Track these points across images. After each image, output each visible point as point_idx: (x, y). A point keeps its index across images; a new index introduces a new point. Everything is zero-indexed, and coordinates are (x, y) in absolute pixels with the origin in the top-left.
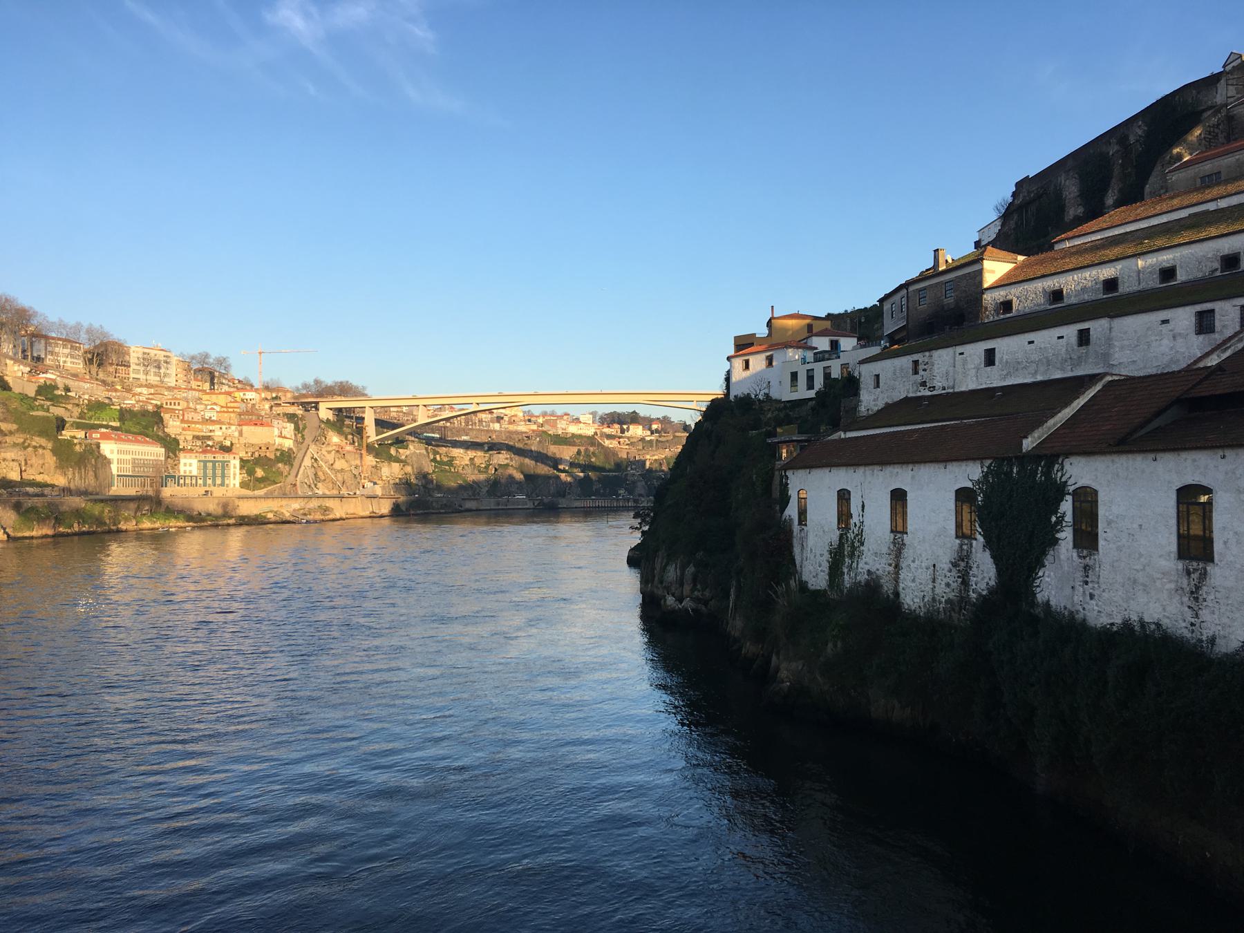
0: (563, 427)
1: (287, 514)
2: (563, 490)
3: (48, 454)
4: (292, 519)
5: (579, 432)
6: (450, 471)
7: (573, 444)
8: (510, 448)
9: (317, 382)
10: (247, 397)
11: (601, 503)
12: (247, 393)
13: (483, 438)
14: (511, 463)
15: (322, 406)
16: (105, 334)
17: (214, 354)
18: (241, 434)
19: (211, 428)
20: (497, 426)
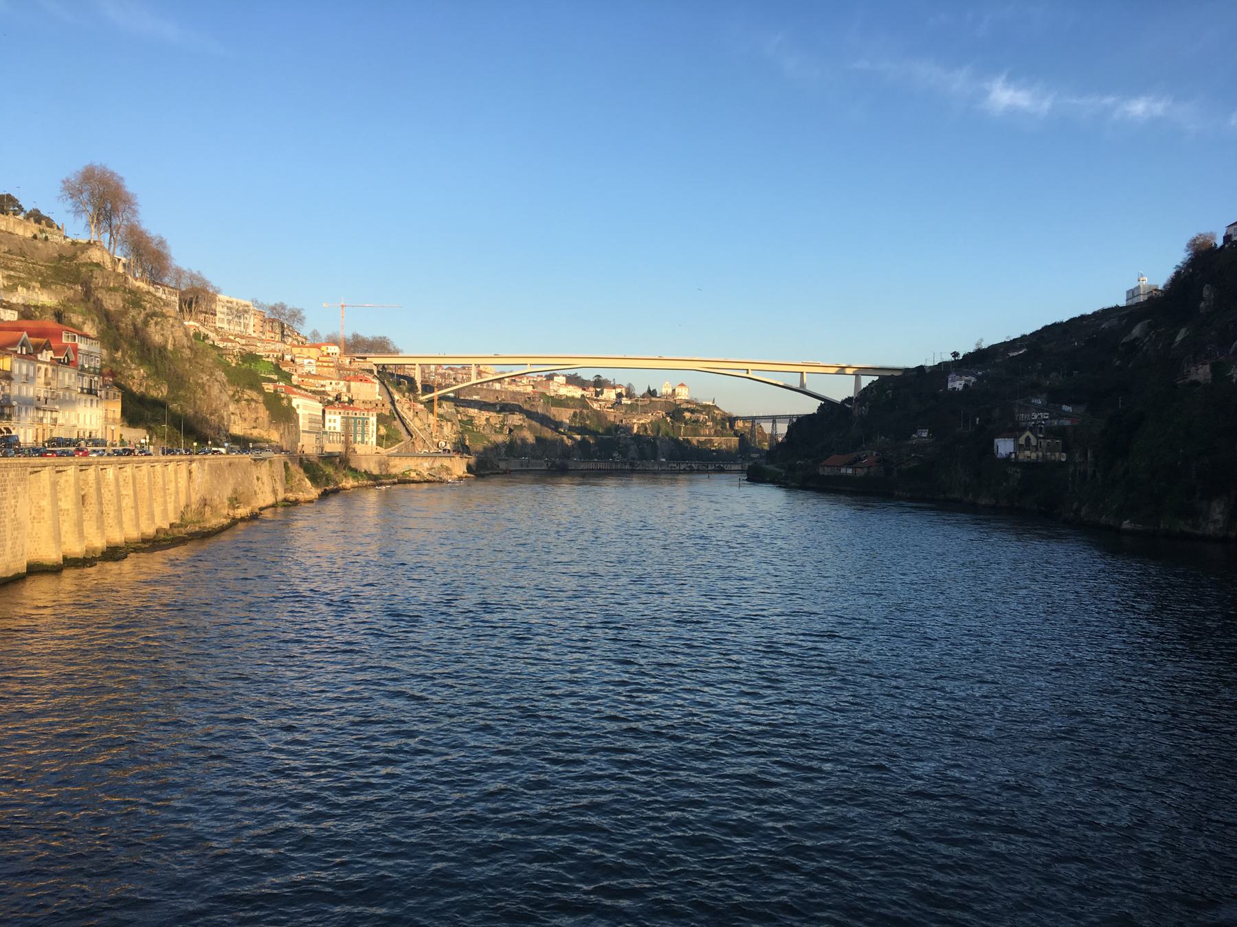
0: (555, 388)
1: (426, 474)
2: (567, 453)
4: (430, 478)
5: (569, 395)
6: (473, 431)
7: (567, 406)
8: (521, 410)
10: (329, 351)
11: (601, 466)
13: (491, 399)
14: (524, 424)
16: (202, 280)
17: (291, 303)
18: (349, 390)
19: (323, 382)
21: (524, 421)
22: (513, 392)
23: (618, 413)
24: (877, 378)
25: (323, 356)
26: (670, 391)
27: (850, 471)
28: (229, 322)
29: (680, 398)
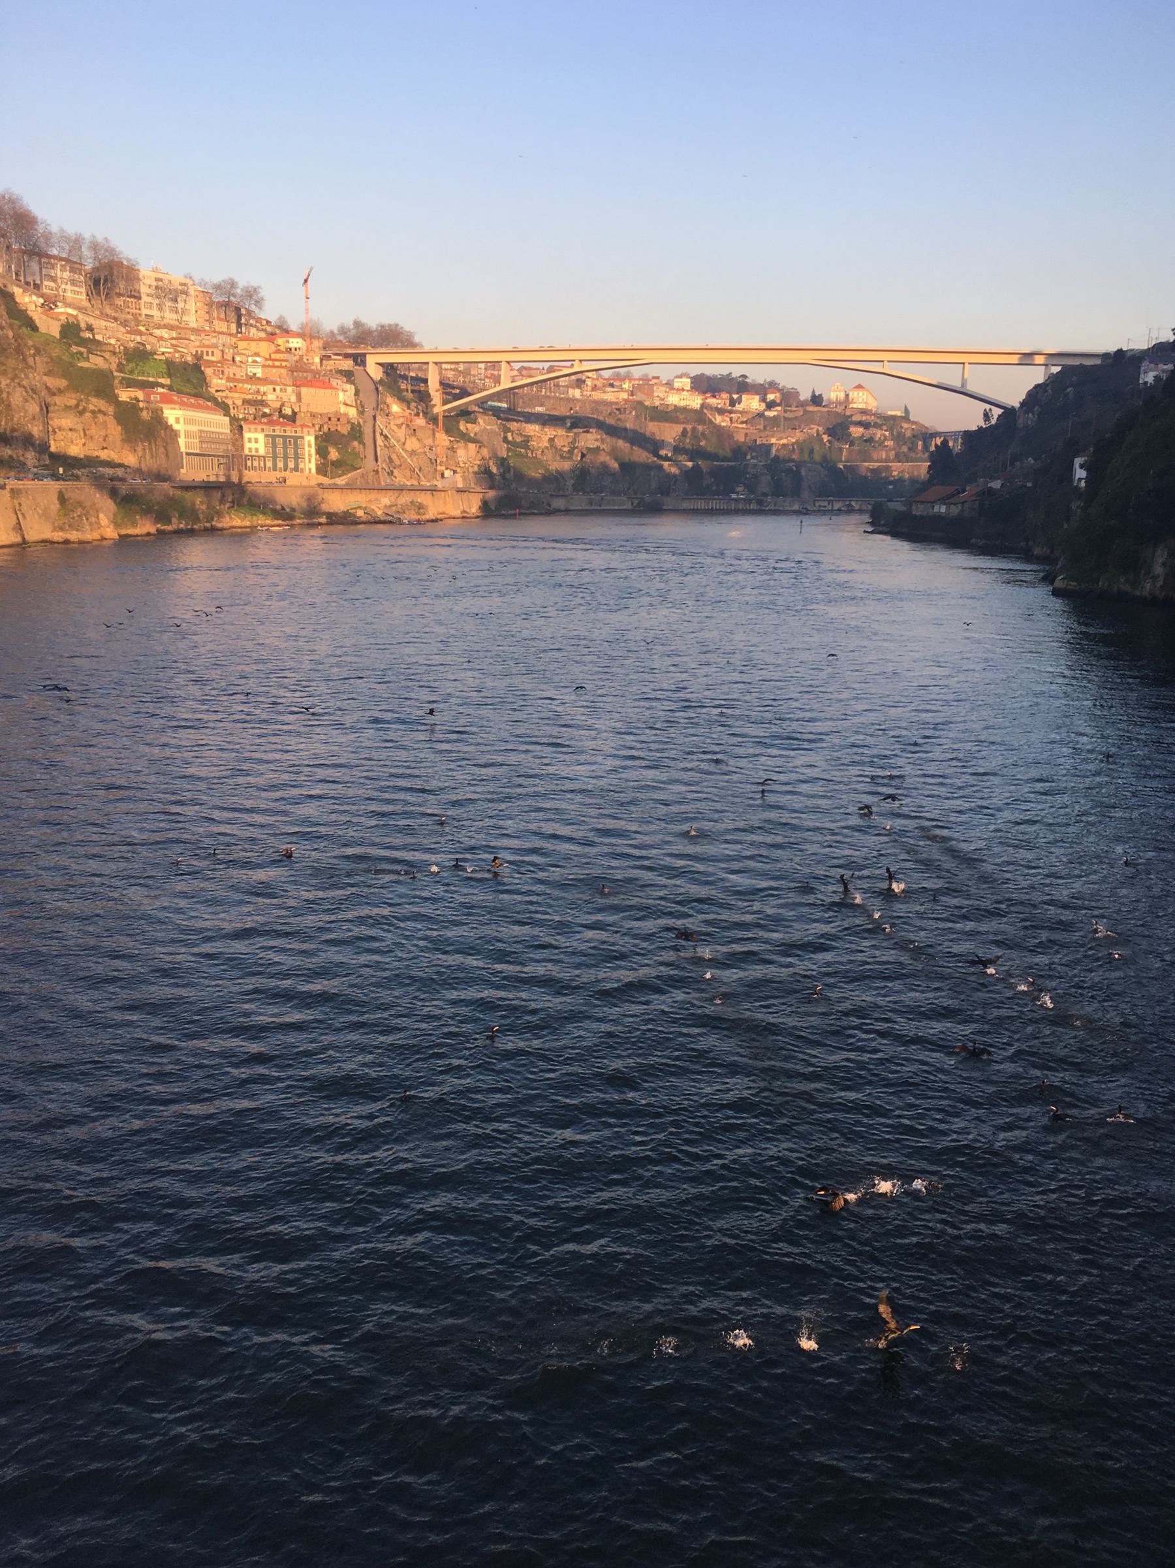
0: (661, 395)
1: (379, 513)
2: (667, 485)
3: (111, 422)
5: (683, 404)
6: (527, 456)
7: (675, 421)
8: (600, 425)
9: (357, 324)
10: (291, 345)
12: (291, 340)
13: (561, 411)
15: (371, 361)
16: (111, 251)
17: (243, 281)
19: (263, 389)
20: (577, 393)
21: (603, 441)
22: (595, 402)
23: (752, 430)
24: (1058, 369)
25: (279, 351)
26: (842, 395)
27: (943, 509)
28: (160, 307)
29: (855, 406)
